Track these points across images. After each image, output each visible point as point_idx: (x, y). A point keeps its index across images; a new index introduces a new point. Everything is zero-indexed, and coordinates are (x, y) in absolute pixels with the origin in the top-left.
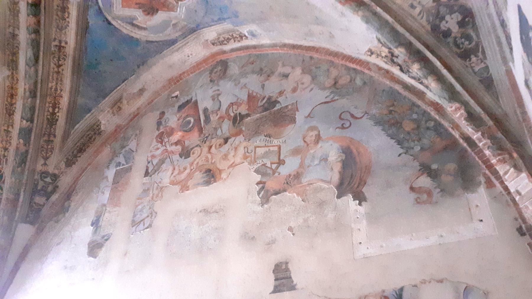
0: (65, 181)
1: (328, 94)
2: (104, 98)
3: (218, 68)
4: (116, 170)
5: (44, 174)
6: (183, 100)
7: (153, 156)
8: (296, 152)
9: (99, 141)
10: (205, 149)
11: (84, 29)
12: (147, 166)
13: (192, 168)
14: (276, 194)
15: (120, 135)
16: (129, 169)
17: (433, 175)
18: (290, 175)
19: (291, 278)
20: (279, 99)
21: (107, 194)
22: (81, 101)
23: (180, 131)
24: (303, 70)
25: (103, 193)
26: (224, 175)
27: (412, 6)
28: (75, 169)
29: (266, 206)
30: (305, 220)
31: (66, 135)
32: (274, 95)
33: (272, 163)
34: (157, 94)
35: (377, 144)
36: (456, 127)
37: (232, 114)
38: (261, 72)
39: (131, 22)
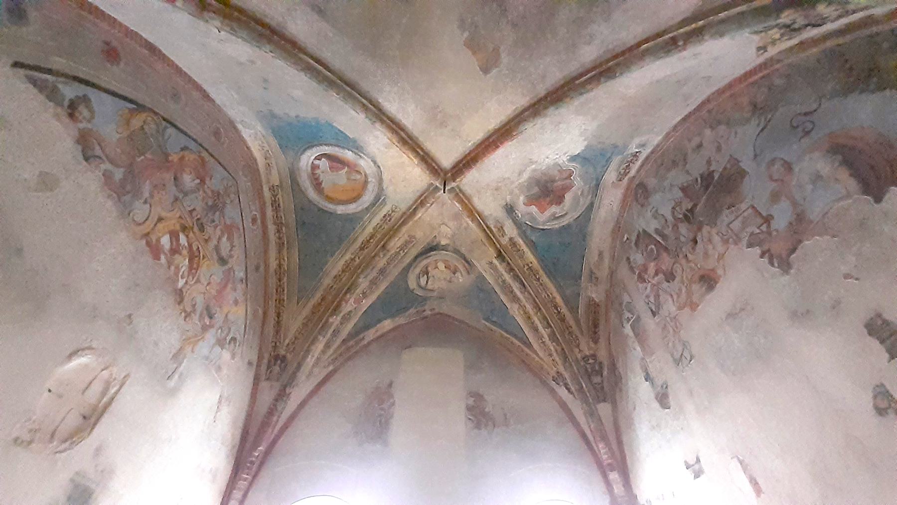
0: (602, 354)
1: (757, 122)
2: (580, 278)
3: (639, 193)
5: (585, 358)
6: (634, 238)
7: (648, 297)
8: (775, 197)
9: (602, 310)
10: (683, 261)
11: (532, 245)
14: (793, 250)
15: (613, 298)
16: (638, 318)
18: (791, 223)
20: (712, 169)
21: (638, 349)
22: (568, 292)
24: (711, 127)
25: (635, 349)
26: (720, 272)
28: (602, 343)
31: (577, 321)
33: (758, 228)
34: (613, 248)
37: (681, 216)
38: (674, 163)
39: (555, 218)
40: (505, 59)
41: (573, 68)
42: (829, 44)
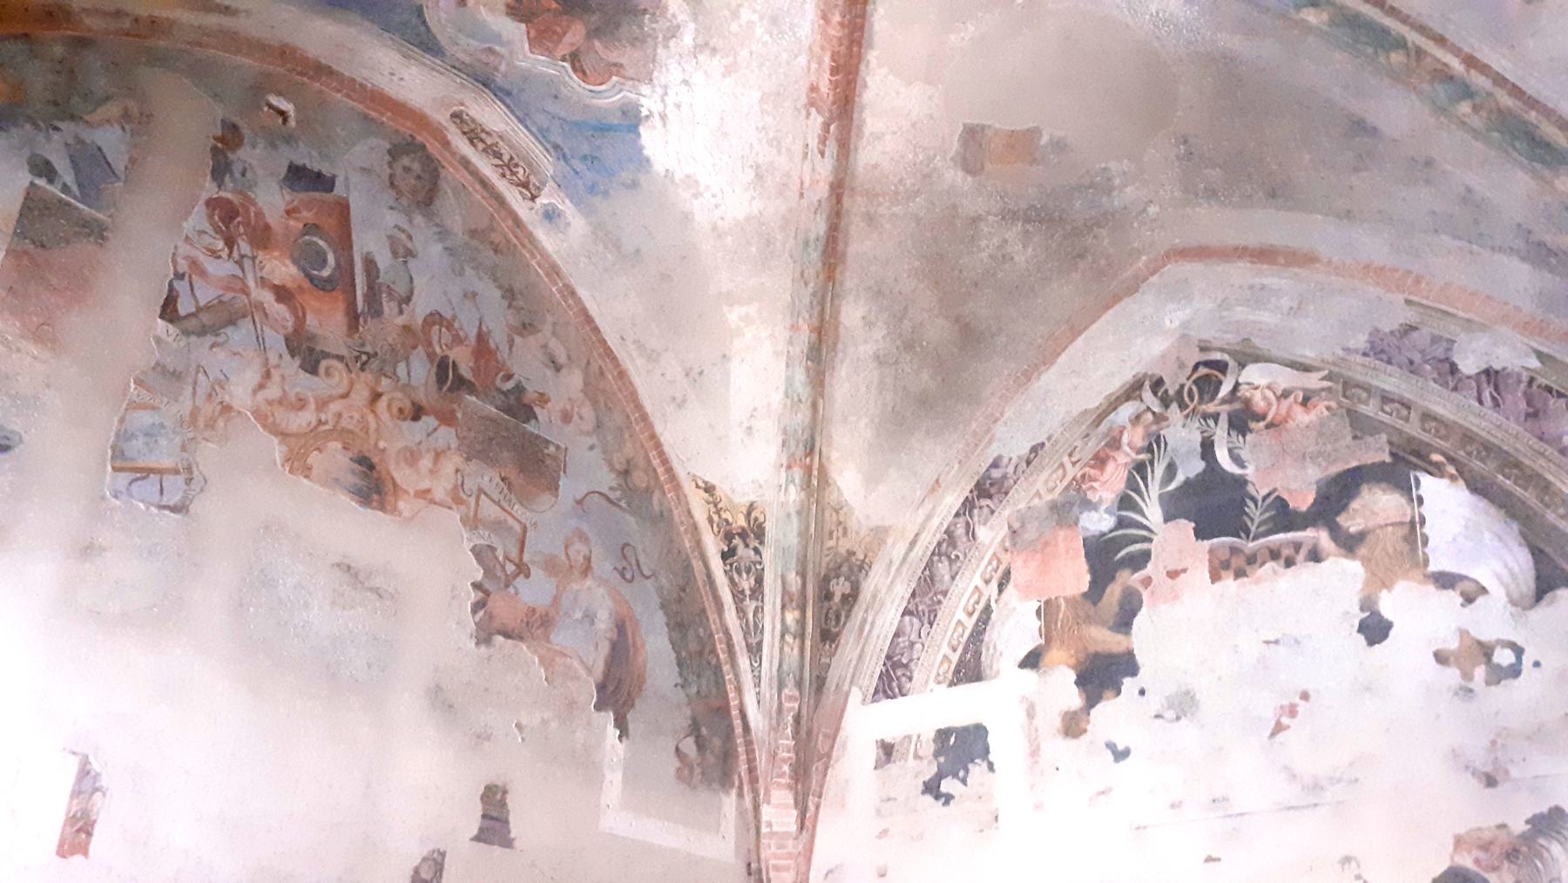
4: (32, 184)
7: (194, 263)
8: (551, 566)
10: (361, 394)
12: (171, 284)
13: (323, 417)
14: (507, 635)
17: (701, 745)
19: (507, 822)
20: (537, 410)
23: (295, 262)
27: (831, 534)
29: (483, 649)
30: (544, 722)
32: (530, 396)
33: (507, 558)
35: (656, 648)
36: (739, 690)
40: (953, 176)
41: (850, 279)
42: (697, 565)
